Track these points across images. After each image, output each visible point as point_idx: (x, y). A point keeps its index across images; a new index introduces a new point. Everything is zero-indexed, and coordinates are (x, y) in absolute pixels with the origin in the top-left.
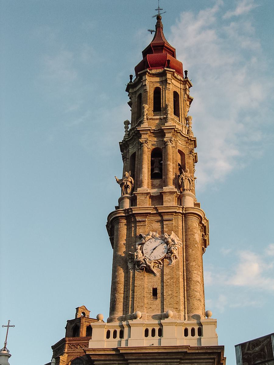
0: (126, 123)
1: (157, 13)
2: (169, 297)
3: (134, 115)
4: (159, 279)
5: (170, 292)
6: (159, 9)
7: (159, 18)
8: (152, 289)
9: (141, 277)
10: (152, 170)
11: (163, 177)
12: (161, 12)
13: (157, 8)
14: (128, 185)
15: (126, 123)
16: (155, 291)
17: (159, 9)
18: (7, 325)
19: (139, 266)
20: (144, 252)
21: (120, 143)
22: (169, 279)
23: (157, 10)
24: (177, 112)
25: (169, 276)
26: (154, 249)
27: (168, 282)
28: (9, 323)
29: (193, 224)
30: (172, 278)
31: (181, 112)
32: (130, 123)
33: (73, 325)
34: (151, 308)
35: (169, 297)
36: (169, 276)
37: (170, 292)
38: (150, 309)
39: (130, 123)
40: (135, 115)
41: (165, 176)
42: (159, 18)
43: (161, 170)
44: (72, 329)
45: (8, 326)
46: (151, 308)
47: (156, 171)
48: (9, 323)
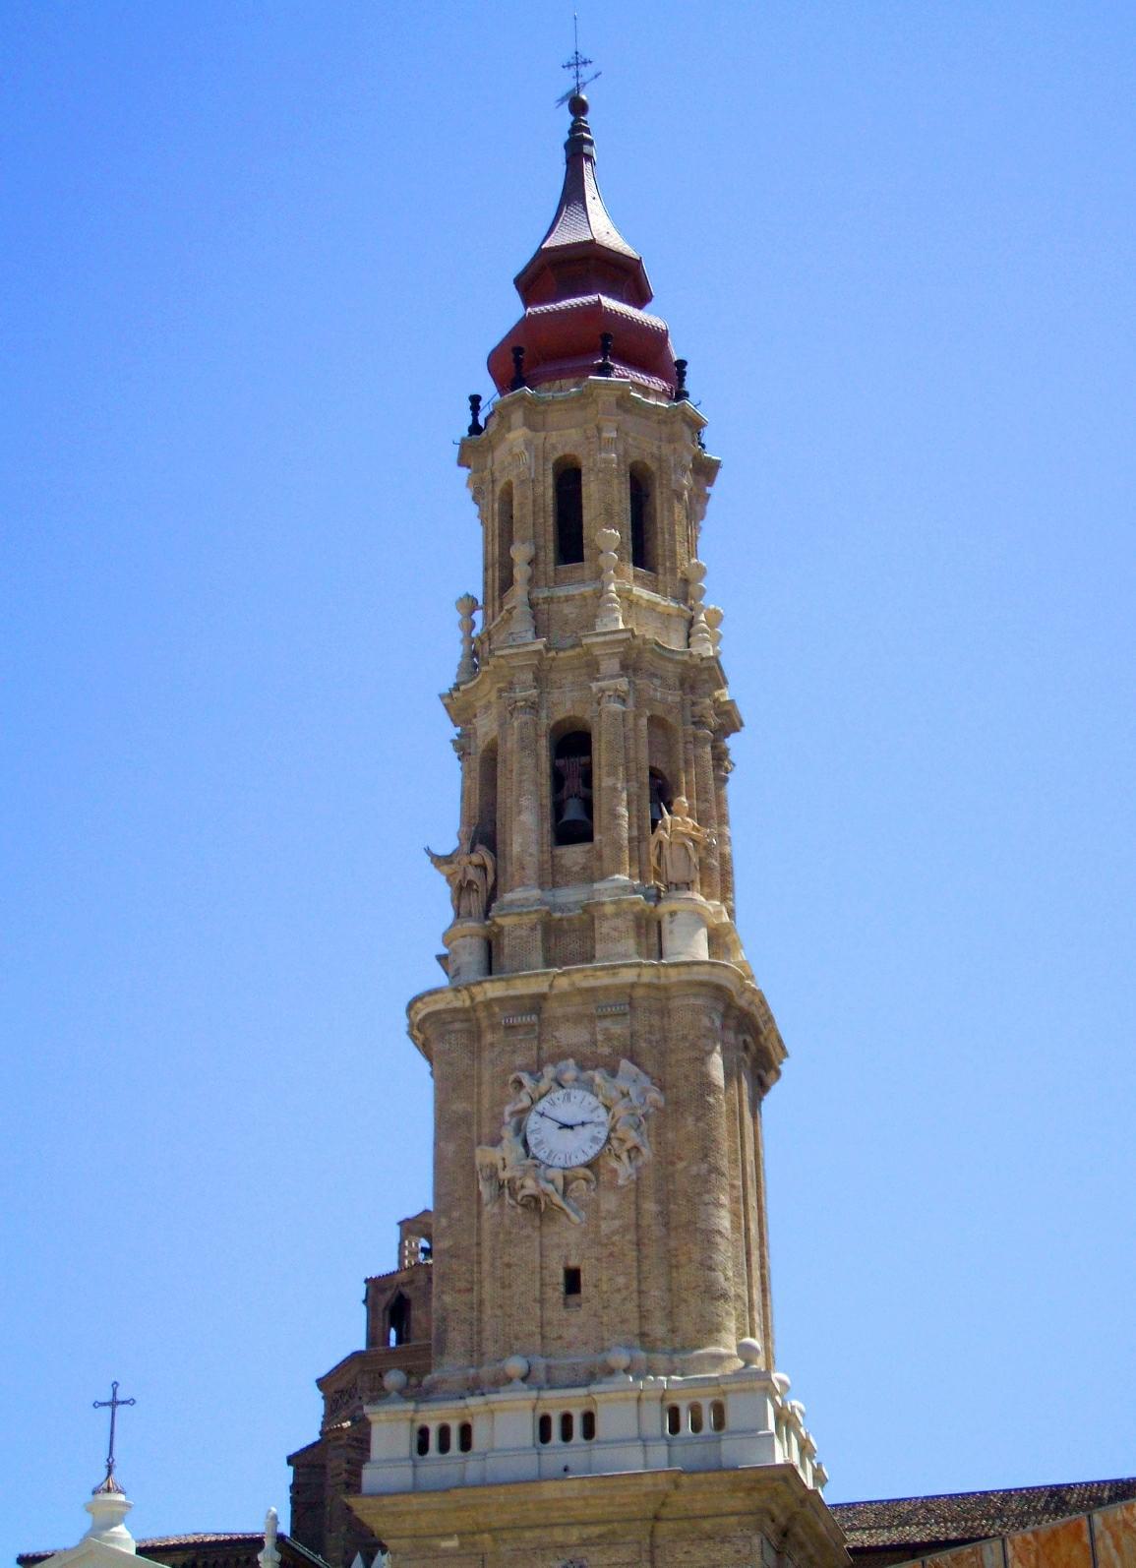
0: (469, 605)
1: (568, 85)
2: (618, 1297)
3: (490, 572)
4: (585, 1234)
5: (621, 1280)
6: (577, 62)
7: (578, 107)
8: (561, 1272)
9: (524, 1232)
10: (558, 809)
11: (597, 837)
12: (586, 72)
13: (568, 57)
14: (470, 883)
15: (469, 605)
16: (573, 1281)
17: (577, 62)
18: (108, 1398)
19: (513, 1194)
20: (532, 1140)
21: (442, 697)
22: (614, 1233)
23: (569, 65)
24: (642, 553)
25: (617, 1223)
26: (571, 1127)
27: (613, 1244)
28: (114, 1394)
29: (700, 1020)
30: (625, 1229)
31: (660, 546)
32: (480, 603)
33: (389, 1294)
34: (560, 1337)
35: (618, 1297)
36: (617, 1223)
37: (621, 1280)
38: (559, 1341)
39: (480, 603)
40: (493, 571)
41: (600, 833)
42: (578, 107)
43: (588, 806)
44: (385, 1309)
45: (114, 1403)
46: (560, 1337)
47: (573, 812)
48: (114, 1394)
